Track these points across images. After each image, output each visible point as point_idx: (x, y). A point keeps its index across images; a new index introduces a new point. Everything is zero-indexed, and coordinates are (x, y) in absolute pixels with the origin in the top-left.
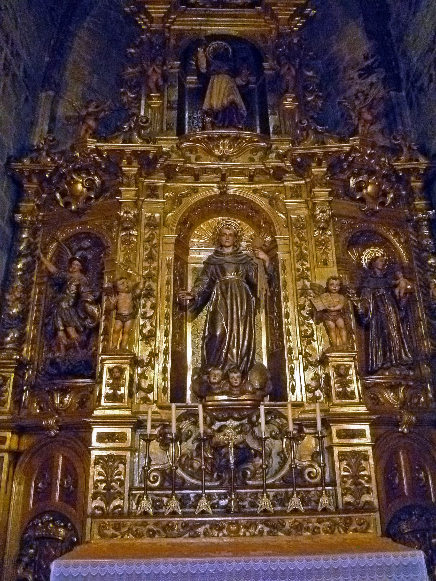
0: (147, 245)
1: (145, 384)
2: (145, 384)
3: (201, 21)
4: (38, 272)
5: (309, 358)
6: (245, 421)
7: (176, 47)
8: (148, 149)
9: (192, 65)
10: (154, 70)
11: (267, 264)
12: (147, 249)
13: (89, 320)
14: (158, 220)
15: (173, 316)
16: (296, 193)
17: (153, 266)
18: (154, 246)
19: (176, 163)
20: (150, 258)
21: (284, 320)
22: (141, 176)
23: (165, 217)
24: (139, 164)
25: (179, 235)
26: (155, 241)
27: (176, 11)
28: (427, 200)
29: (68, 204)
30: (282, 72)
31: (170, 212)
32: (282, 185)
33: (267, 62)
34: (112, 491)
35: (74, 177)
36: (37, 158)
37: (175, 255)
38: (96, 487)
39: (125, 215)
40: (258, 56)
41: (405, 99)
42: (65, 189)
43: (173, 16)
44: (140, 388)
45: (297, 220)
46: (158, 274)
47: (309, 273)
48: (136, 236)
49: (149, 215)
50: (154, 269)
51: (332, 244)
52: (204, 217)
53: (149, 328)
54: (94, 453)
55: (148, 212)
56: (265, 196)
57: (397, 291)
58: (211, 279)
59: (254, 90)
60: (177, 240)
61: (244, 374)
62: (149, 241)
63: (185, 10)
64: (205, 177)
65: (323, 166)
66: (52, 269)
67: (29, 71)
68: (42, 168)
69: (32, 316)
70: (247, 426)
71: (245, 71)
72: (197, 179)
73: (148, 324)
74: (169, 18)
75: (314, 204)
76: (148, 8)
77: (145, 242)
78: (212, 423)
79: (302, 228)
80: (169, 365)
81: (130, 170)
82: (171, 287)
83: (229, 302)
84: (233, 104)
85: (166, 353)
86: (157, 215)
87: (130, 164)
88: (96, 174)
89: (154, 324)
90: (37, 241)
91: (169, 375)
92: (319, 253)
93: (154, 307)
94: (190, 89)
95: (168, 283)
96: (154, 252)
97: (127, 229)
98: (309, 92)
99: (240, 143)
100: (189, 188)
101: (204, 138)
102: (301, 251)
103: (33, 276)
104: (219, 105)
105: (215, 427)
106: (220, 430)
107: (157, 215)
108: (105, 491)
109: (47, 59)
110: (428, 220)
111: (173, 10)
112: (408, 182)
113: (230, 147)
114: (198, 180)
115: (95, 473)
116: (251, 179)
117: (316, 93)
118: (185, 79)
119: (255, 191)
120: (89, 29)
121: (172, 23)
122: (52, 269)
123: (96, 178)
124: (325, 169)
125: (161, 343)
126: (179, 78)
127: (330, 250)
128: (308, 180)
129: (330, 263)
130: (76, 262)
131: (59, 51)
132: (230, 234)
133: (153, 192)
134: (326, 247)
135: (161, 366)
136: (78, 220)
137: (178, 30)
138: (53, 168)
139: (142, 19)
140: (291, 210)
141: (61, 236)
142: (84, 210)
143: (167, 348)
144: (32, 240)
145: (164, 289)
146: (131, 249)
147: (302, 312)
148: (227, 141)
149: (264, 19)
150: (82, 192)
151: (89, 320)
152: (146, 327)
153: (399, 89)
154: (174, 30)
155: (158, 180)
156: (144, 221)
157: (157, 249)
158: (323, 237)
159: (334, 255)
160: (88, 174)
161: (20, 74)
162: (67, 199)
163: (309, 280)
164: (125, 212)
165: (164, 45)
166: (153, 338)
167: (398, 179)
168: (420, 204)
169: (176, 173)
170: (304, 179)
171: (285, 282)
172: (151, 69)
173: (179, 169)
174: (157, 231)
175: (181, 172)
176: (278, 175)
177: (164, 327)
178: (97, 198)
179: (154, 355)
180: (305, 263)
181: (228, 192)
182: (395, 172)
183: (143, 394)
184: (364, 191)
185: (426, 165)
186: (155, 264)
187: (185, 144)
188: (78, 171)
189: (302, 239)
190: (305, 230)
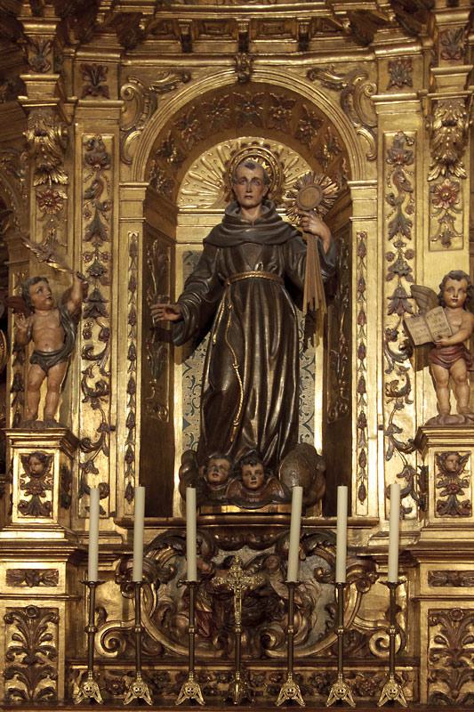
5: (395, 436)
6: (271, 550)
11: (326, 246)
14: (109, 150)
15: (144, 352)
17: (102, 250)
18: (102, 208)
20: (97, 233)
21: (355, 361)
23: (122, 142)
25: (154, 183)
26: (104, 197)
31: (134, 129)
32: (370, 57)
37: (145, 224)
47: (410, 263)
53: (98, 377)
56: (332, 86)
60: (150, 192)
61: (272, 467)
70: (273, 558)
72: (187, 49)
73: (96, 371)
78: (213, 553)
79: (405, 162)
80: (137, 449)
83: (247, 326)
85: (131, 424)
86: (106, 138)
89: (107, 369)
91: (136, 466)
92: (435, 220)
93: (105, 336)
95: (132, 287)
96: (103, 221)
102: (400, 215)
105: (218, 560)
106: (226, 565)
116: (304, 46)
119: (313, 74)
125: (123, 405)
127: (458, 211)
128: (428, 43)
129: (456, 242)
132: (254, 179)
134: (452, 205)
135: (123, 449)
143: (132, 415)
145: (124, 300)
152: (92, 376)
156: (80, 151)
158: (447, 183)
163: (409, 279)
166: (106, 398)
169: (142, 37)
170: (419, 41)
173: (147, 25)
174: (108, 174)
175: (153, 32)
179: (107, 429)
180: (404, 240)
189: (404, 187)
190: (412, 167)
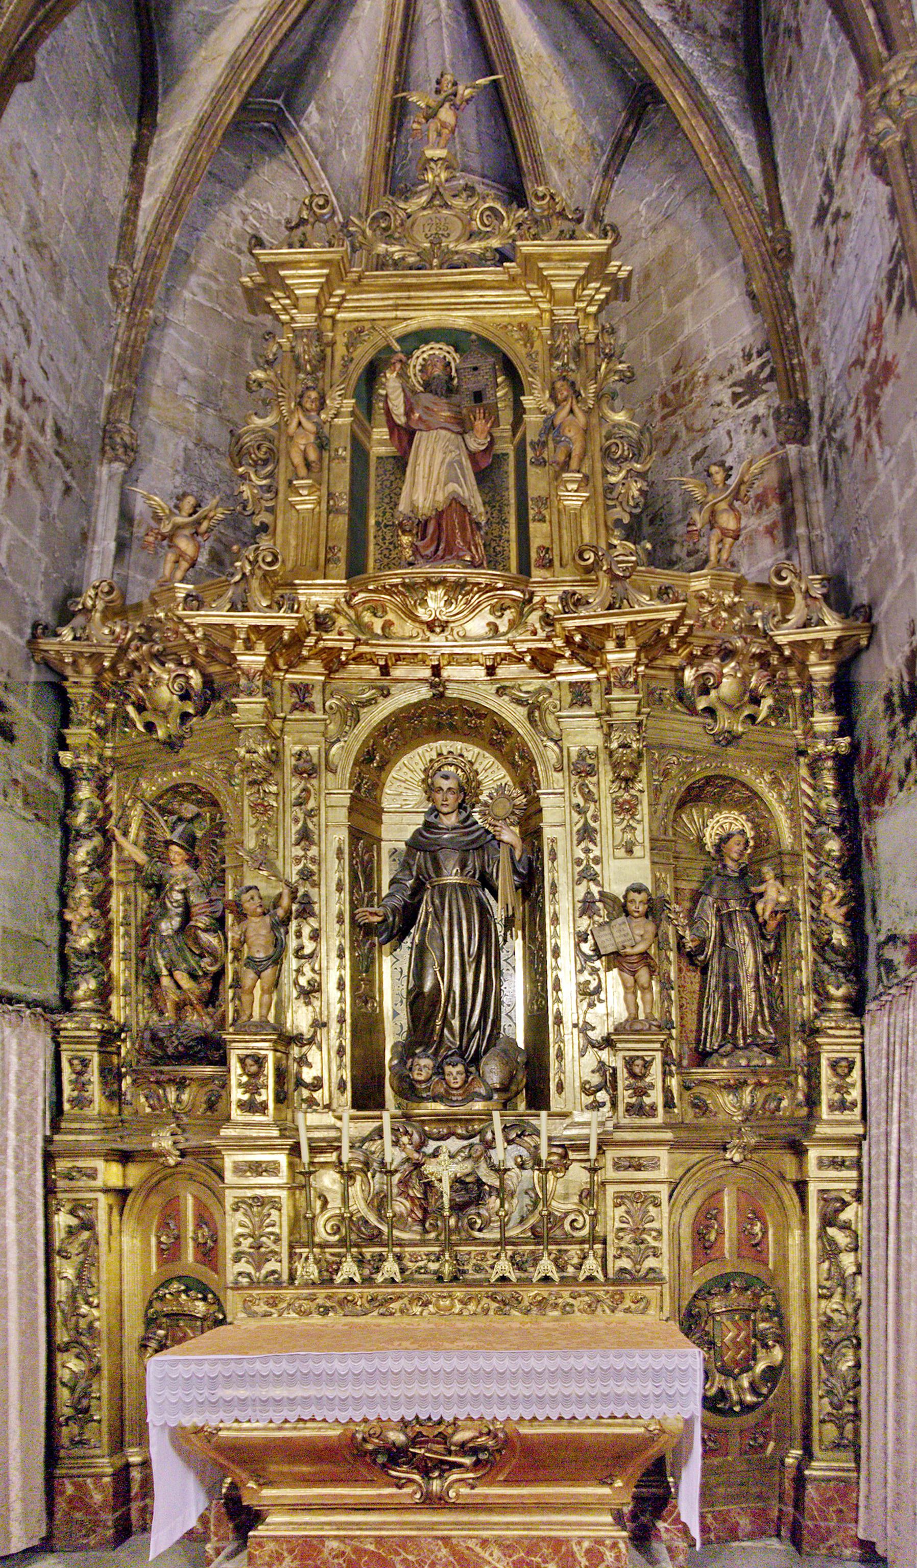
1: (308, 1075)
2: (308, 1075)
4: (119, 861)
11: (517, 855)
15: (353, 949)
18: (309, 814)
20: (305, 837)
22: (277, 669)
23: (327, 754)
25: (358, 788)
26: (311, 804)
29: (150, 727)
31: (338, 740)
42: (140, 698)
44: (300, 1083)
47: (597, 868)
49: (298, 748)
51: (644, 809)
53: (309, 975)
55: (295, 743)
58: (417, 878)
60: (353, 798)
62: (301, 804)
66: (141, 857)
69: (119, 944)
73: (307, 969)
80: (347, 1044)
81: (253, 660)
82: (346, 895)
83: (446, 929)
85: (341, 1021)
86: (313, 749)
88: (193, 664)
90: (108, 799)
96: (311, 826)
103: (110, 869)
122: (141, 857)
127: (639, 822)
129: (638, 850)
135: (335, 1044)
136: (173, 759)
141: (149, 788)
142: (181, 738)
143: (343, 1011)
144: (98, 802)
145: (332, 902)
150: (170, 703)
156: (290, 762)
157: (315, 819)
160: (180, 664)
162: (149, 716)
170: (595, 670)
179: (319, 1024)
180: (591, 846)
183: (306, 1093)
186: (313, 851)
188: (160, 658)
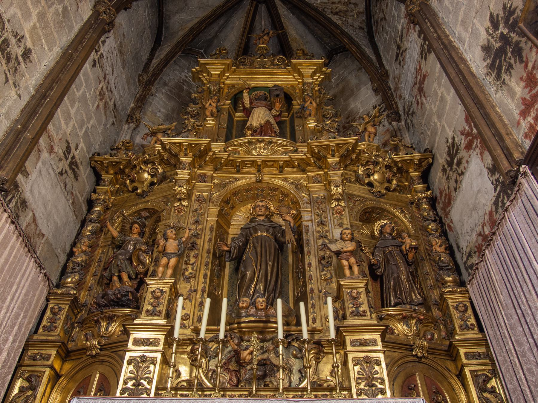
0: (195, 213)
3: (247, 78)
7: (227, 93)
8: (201, 142)
9: (240, 107)
10: (210, 104)
12: (194, 216)
13: (141, 266)
16: (316, 180)
17: (198, 227)
18: (201, 215)
19: (222, 156)
20: (197, 222)
24: (193, 156)
27: (228, 70)
28: (424, 184)
30: (306, 106)
32: (305, 176)
33: (296, 101)
34: (140, 387)
35: (142, 167)
36: (115, 154)
38: (125, 383)
39: (179, 189)
40: (288, 99)
41: (404, 126)
43: (226, 74)
45: (317, 198)
46: (202, 233)
47: (328, 234)
48: (187, 207)
50: (199, 229)
51: (346, 213)
52: (243, 202)
54: (128, 355)
57: (403, 247)
58: (246, 238)
59: (285, 121)
63: (235, 70)
64: (246, 169)
65: (336, 156)
67: (117, 105)
68: (118, 160)
71: (277, 105)
72: (238, 172)
74: (224, 76)
75: (330, 182)
76: (210, 68)
77: (193, 211)
82: (212, 244)
84: (268, 121)
86: (205, 194)
87: (186, 155)
93: (196, 257)
94: (238, 121)
95: (210, 240)
96: (200, 219)
97: (180, 200)
98: (327, 118)
99: (272, 146)
100: (232, 177)
101: (245, 143)
102: (321, 219)
104: (258, 124)
107: (205, 194)
108: (133, 387)
109: (132, 105)
110: (426, 198)
111: (226, 70)
112: (407, 172)
113: (265, 149)
114: (239, 172)
115: (126, 370)
117: (332, 119)
118: (234, 115)
120: (166, 94)
121: (226, 79)
123: (159, 167)
124: (338, 159)
126: (229, 113)
127: (344, 217)
130: (136, 225)
131: (142, 101)
133: (203, 178)
137: (230, 84)
138: (127, 161)
139: (204, 76)
140: (312, 191)
145: (205, 244)
146: (182, 216)
147: (323, 262)
148: (262, 145)
149: (294, 76)
151: (141, 266)
152: (187, 271)
153: (399, 120)
154: (228, 84)
155: (208, 171)
157: (203, 217)
159: (348, 220)
161: (111, 104)
164: (179, 187)
165: (220, 90)
167: (400, 170)
168: (419, 187)
169: (221, 168)
170: (323, 170)
171: (308, 240)
172: (208, 104)
174: (204, 205)
176: (302, 166)
177: (202, 272)
178: (160, 182)
181: (263, 181)
182: (396, 164)
184: (372, 178)
185: (420, 157)
187: (231, 148)
